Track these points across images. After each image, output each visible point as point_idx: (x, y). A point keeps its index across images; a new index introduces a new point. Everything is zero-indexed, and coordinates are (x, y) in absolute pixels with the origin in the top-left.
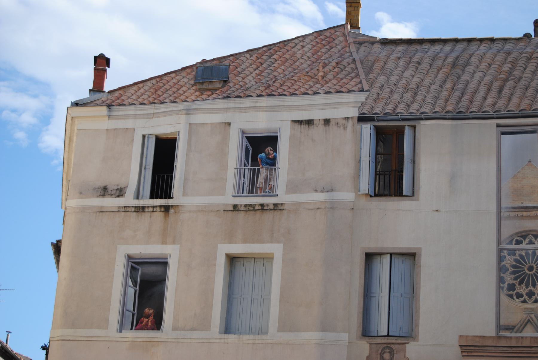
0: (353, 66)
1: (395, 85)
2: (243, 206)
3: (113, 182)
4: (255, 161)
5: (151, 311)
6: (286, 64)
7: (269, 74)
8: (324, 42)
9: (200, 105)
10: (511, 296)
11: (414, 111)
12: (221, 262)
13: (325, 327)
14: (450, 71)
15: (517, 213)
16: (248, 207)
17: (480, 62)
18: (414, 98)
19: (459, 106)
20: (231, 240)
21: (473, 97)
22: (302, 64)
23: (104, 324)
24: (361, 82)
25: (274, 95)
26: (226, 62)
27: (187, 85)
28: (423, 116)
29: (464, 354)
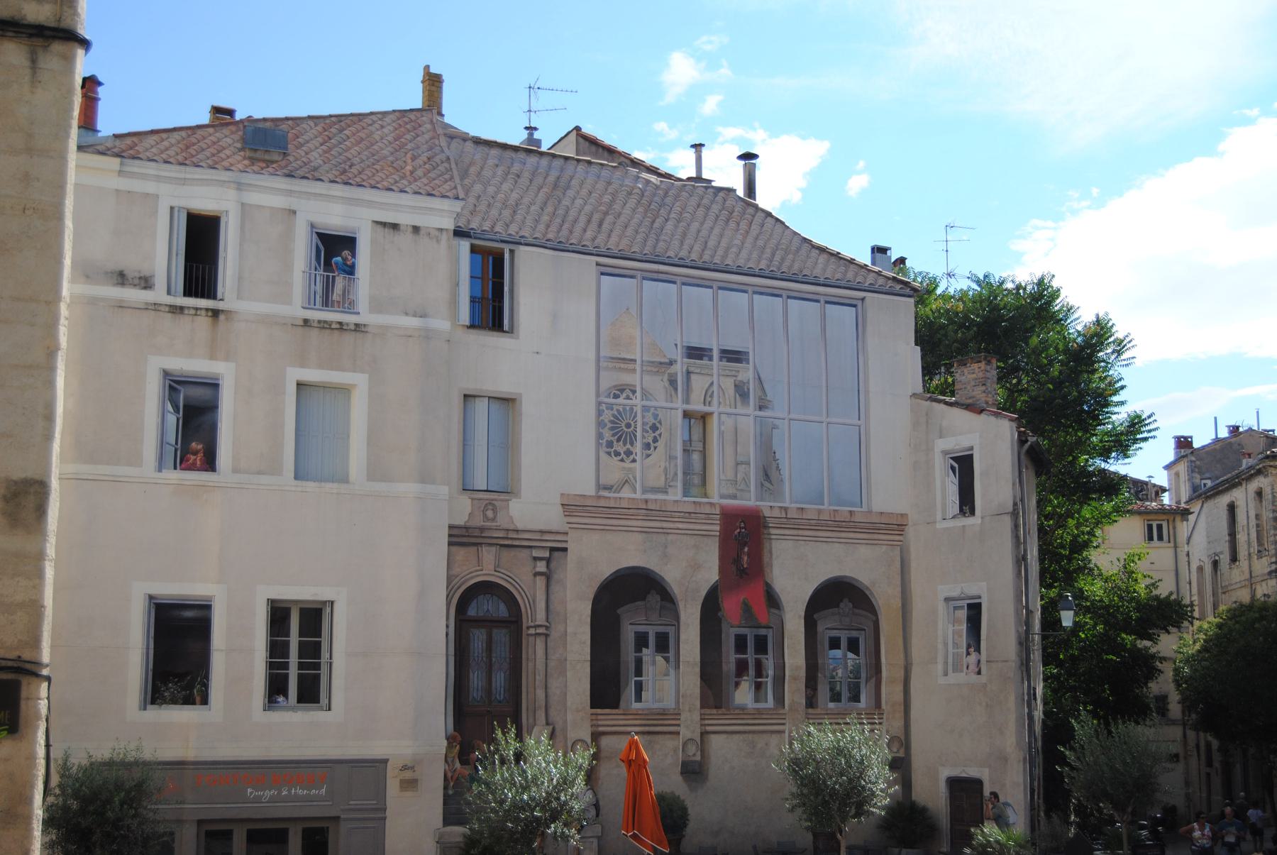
0: (446, 165)
1: (493, 197)
2: (316, 321)
3: (132, 264)
4: (328, 266)
5: (200, 447)
7: (340, 154)
8: (408, 126)
9: (249, 178)
10: (609, 454)
11: (513, 233)
12: (291, 389)
13: (425, 478)
14: (552, 192)
15: (614, 364)
16: (322, 324)
17: (581, 187)
18: (512, 217)
19: (560, 235)
20: (303, 365)
21: (573, 226)
22: (382, 149)
23: (134, 459)
24: (455, 188)
25: (351, 184)
26: (284, 127)
27: (232, 148)
29: (566, 513)
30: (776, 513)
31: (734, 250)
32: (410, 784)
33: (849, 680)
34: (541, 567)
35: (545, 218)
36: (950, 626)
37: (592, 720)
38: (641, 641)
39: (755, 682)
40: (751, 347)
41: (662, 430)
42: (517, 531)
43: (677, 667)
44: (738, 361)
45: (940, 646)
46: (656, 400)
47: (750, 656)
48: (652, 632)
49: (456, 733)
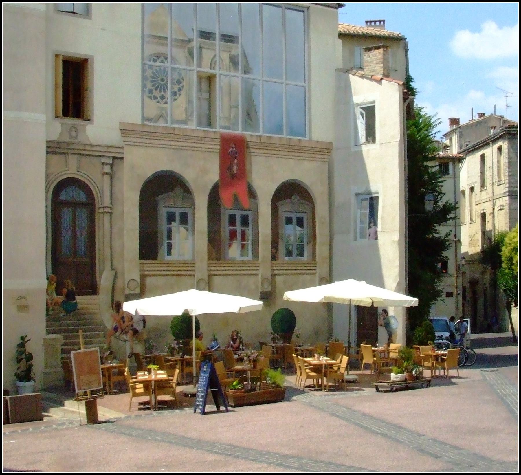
10: (150, 98)
29: (123, 135)
30: (254, 139)
32: (23, 308)
34: (107, 169)
36: (359, 211)
38: (171, 218)
41: (184, 83)
42: (91, 145)
44: (231, 41)
45: (352, 223)
47: (238, 228)
48: (178, 212)
49: (53, 276)
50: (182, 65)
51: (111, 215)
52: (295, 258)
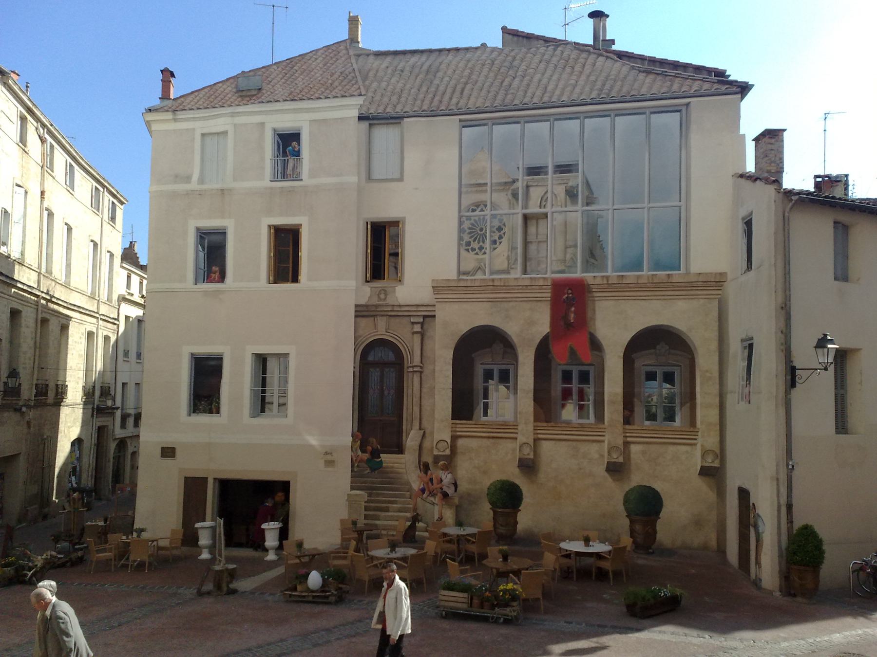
0: (353, 74)
4: (285, 154)
5: (217, 269)
6: (305, 74)
8: (332, 55)
10: (468, 250)
11: (400, 111)
14: (425, 76)
17: (447, 68)
21: (442, 98)
22: (316, 73)
24: (359, 88)
25: (296, 100)
28: (405, 115)
30: (598, 281)
31: (569, 88)
33: (664, 404)
34: (417, 328)
35: (421, 96)
37: (452, 427)
38: (488, 375)
39: (579, 404)
40: (580, 159)
41: (506, 229)
42: (400, 306)
43: (516, 392)
44: (569, 171)
46: (502, 209)
47: (575, 386)
48: (496, 369)
50: (504, 209)
51: (421, 374)
52: (659, 423)
